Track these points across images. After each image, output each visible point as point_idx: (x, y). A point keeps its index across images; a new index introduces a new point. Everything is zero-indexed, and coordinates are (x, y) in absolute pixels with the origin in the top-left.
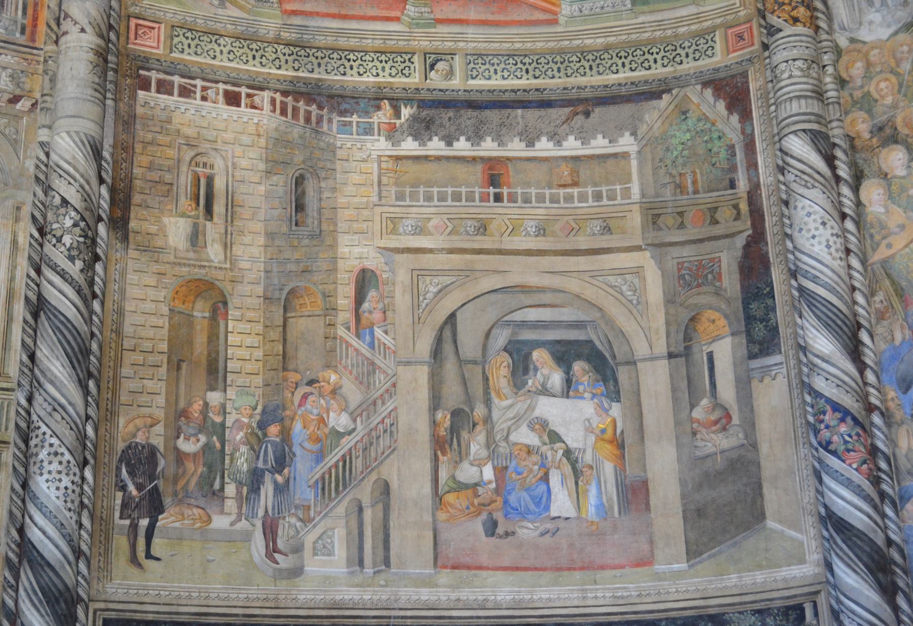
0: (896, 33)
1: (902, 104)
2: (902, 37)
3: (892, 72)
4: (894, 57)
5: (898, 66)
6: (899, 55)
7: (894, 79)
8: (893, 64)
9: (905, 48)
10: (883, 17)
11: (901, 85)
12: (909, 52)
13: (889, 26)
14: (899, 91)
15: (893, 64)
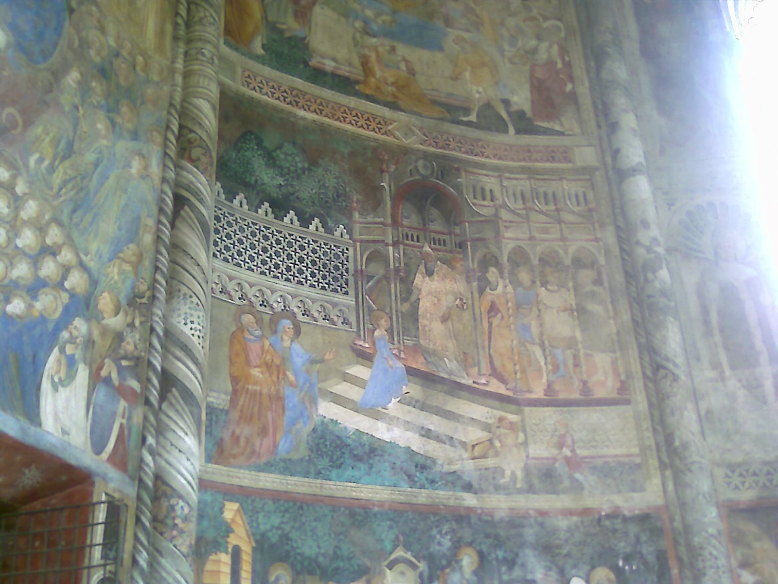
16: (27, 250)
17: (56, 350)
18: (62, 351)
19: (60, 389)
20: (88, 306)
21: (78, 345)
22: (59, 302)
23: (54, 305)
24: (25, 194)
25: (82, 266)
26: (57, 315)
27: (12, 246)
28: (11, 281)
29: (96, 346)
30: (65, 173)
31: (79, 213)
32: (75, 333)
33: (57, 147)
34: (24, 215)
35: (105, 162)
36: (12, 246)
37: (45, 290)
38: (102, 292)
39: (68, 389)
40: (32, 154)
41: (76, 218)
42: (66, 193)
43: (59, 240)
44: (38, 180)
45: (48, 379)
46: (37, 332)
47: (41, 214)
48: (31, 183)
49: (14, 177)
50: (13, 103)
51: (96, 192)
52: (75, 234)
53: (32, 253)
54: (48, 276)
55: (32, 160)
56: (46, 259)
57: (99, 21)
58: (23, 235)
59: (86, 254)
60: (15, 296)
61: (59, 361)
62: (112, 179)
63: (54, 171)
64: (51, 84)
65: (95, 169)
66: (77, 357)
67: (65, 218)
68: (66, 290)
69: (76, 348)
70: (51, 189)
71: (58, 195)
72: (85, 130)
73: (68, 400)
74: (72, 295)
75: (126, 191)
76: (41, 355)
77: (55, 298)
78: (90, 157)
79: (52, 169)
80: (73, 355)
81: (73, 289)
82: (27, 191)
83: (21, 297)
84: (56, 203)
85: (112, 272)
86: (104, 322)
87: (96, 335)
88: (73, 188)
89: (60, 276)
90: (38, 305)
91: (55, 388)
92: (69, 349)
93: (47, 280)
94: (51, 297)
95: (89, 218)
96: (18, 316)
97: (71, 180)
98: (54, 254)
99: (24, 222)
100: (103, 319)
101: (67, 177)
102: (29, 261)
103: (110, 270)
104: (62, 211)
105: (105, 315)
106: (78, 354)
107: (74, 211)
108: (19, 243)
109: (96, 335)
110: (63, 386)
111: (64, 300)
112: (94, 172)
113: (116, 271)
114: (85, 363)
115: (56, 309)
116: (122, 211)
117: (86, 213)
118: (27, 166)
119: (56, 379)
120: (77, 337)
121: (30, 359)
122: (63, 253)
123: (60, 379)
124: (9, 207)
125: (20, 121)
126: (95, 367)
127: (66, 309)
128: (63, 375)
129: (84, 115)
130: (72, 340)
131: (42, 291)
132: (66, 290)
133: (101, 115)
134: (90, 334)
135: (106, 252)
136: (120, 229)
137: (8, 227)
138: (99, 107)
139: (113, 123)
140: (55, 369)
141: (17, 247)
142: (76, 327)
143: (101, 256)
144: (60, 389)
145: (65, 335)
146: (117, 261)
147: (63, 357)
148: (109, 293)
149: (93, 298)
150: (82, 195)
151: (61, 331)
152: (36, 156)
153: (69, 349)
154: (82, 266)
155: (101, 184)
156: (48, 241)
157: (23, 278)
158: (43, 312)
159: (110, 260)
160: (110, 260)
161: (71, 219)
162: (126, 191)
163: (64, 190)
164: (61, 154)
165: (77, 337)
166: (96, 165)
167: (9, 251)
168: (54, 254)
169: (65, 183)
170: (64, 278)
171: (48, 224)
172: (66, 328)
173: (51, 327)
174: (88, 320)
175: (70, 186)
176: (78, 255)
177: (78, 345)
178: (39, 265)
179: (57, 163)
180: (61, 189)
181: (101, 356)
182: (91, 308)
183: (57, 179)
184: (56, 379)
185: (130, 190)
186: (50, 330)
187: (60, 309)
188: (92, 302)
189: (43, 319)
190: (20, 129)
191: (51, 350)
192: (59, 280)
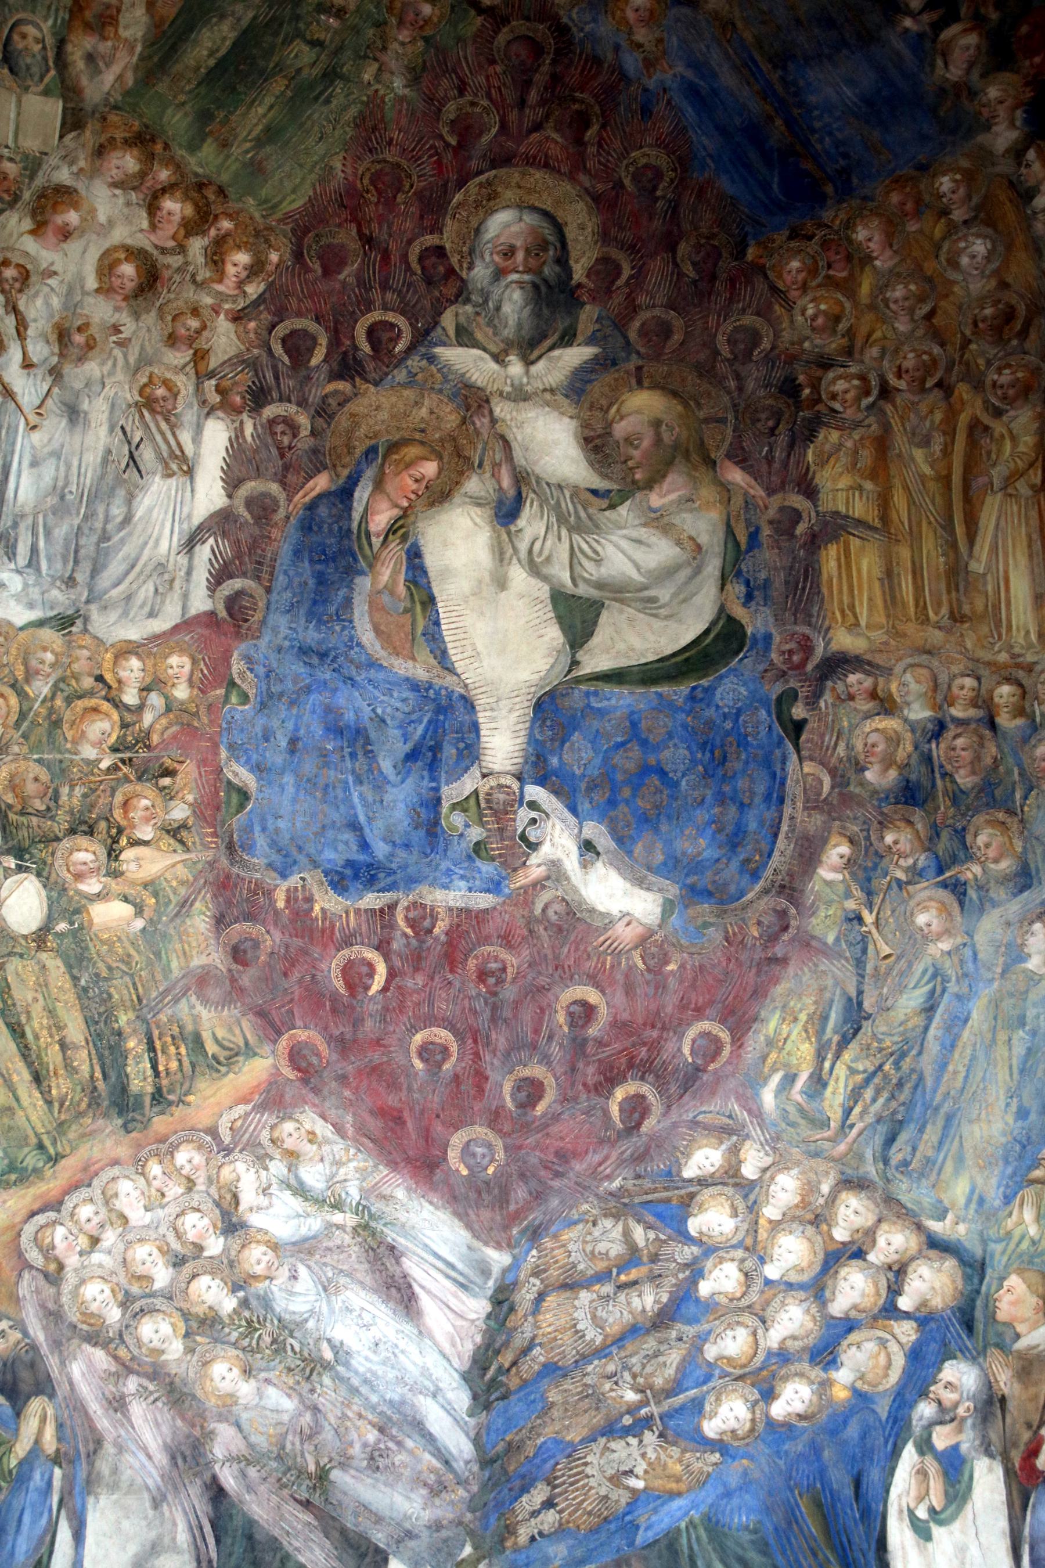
0: (40, 623)
1: (16, 749)
2: (47, 634)
3: (13, 686)
4: (26, 663)
5: (27, 680)
6: (34, 663)
7: (14, 700)
8: (20, 674)
9: (49, 657)
10: (26, 585)
11: (23, 715)
12: (53, 666)
13: (31, 606)
14: (18, 725)
15: (20, 674)
16: (794, 1278)
17: (909, 1455)
18: (925, 1446)
19: (937, 1531)
20: (969, 1326)
21: (963, 1420)
22: (893, 1347)
23: (882, 1360)
24: (765, 1170)
25: (936, 1245)
26: (894, 1376)
27: (758, 1286)
28: (770, 1354)
29: (1011, 1405)
30: (853, 1071)
31: (903, 1137)
32: (949, 1397)
33: (822, 1031)
34: (771, 1212)
35: (952, 987)
36: (758, 1286)
37: (853, 1337)
38: (1002, 1279)
39: (956, 1526)
40: (766, 1080)
41: (896, 1156)
42: (864, 1112)
43: (866, 1219)
44: (793, 1125)
45: (901, 1519)
46: (852, 1431)
47: (810, 1189)
48: (773, 1142)
49: (735, 1151)
50: (699, 1012)
51: (943, 1066)
52: (905, 1190)
53: (805, 1278)
54: (855, 1307)
55: (768, 1097)
56: (843, 1272)
57: (873, 695)
58: (776, 1251)
59: (941, 1217)
60: (786, 1379)
61: (922, 1473)
62: (978, 1013)
63: (825, 1085)
64: (783, 914)
65: (930, 1019)
66: (964, 1447)
67: (871, 1170)
68: (907, 1315)
69: (960, 1430)
70: (825, 1124)
71: (845, 1126)
72: (886, 950)
73: (962, 1550)
74: (923, 1318)
75: (1022, 1022)
76: (874, 1475)
77: (883, 1343)
78: (911, 1001)
79: (819, 1082)
80: (956, 1448)
81: (924, 1303)
82: (769, 1160)
83: (801, 1375)
84: (842, 1148)
85: (1021, 1222)
86: (1021, 1345)
87: (1005, 1380)
88: (878, 1092)
89: (884, 1293)
90: (843, 1376)
91: (922, 1532)
92: (942, 1439)
93: (853, 1314)
94: (870, 1346)
95: (932, 1134)
96: (800, 1416)
97: (867, 1081)
98: (859, 1254)
99: (776, 1226)
100: (1018, 1336)
101: (859, 1078)
102: (802, 1295)
103: (1010, 1223)
104: (861, 1157)
105: (1020, 1328)
106: (968, 1441)
107: (890, 1140)
108: (772, 1272)
109: (1005, 1380)
110: (941, 1523)
111: (904, 1339)
112: (926, 1029)
113: (1028, 1215)
114: (991, 1456)
115: (889, 1365)
116: (1022, 1071)
117: (921, 1130)
118: (757, 1113)
119: (922, 1513)
120: (956, 1405)
121: (849, 1492)
122: (881, 1242)
123: (932, 1511)
124: (735, 1214)
125: (725, 1036)
126: (1016, 1457)
127: (915, 1355)
128: (936, 1499)
129: (877, 923)
130: (946, 1415)
131: (845, 1343)
132: (907, 1315)
133: (924, 891)
134: (989, 1385)
135: (992, 1188)
136: (1022, 1114)
137: (740, 1253)
138: (916, 874)
139: (958, 889)
140: (913, 1493)
141: (768, 1282)
142: (949, 1385)
143: (981, 1201)
144: (937, 1531)
145: (925, 1410)
146: (1029, 1193)
147: (929, 1460)
148: (1020, 1272)
149: (979, 1303)
150: (904, 1096)
151: (912, 1405)
152: (776, 1078)
153: (942, 1439)
154: (936, 1245)
155: (951, 1045)
156: (840, 1234)
157: (794, 1338)
158: (859, 1385)
159: (1008, 1200)
160: (1008, 1200)
161: (886, 1162)
162: (1022, 1022)
163: (857, 1110)
164: (836, 1038)
165: (956, 1405)
166: (929, 1009)
167: (754, 1297)
168: (859, 1254)
169: (855, 1095)
170: (895, 1290)
171: (832, 1199)
172: (924, 1394)
173: (883, 1409)
174: (975, 1357)
175: (868, 1094)
176: (919, 1227)
177: (963, 1420)
178: (828, 1294)
179: (827, 1065)
180: (848, 1112)
181: (1029, 1426)
182: (979, 1327)
183: (835, 1097)
184: (922, 1513)
185: (1031, 1013)
186: (884, 1415)
187: (899, 1361)
188: (979, 1314)
189: (861, 1398)
190: (726, 1052)
191: (895, 1454)
192: (881, 1301)
